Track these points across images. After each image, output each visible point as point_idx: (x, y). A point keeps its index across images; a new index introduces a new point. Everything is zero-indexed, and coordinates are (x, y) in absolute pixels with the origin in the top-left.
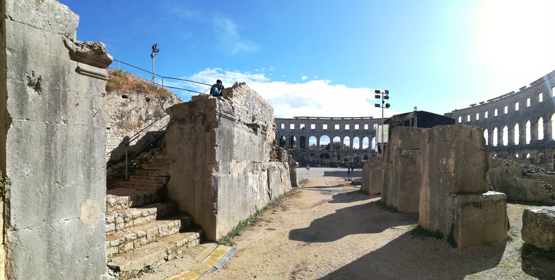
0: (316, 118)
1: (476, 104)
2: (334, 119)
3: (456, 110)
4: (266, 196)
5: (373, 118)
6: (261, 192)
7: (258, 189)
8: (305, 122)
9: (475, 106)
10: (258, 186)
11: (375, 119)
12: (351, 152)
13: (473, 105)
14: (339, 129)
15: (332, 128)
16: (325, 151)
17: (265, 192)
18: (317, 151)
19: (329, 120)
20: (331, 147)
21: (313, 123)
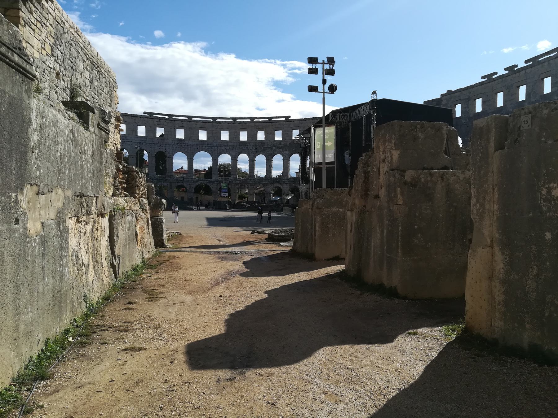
0: (187, 118)
1: (496, 73)
2: (218, 120)
3: (449, 92)
4: (106, 270)
5: (290, 119)
6: (96, 263)
7: (89, 258)
8: (165, 124)
9: (494, 77)
10: (90, 251)
11: (293, 120)
12: (250, 182)
13: (489, 76)
14: (228, 139)
15: (215, 138)
16: (203, 182)
17: (105, 263)
18: (188, 181)
19: (209, 122)
20: (214, 174)
21: (180, 128)
